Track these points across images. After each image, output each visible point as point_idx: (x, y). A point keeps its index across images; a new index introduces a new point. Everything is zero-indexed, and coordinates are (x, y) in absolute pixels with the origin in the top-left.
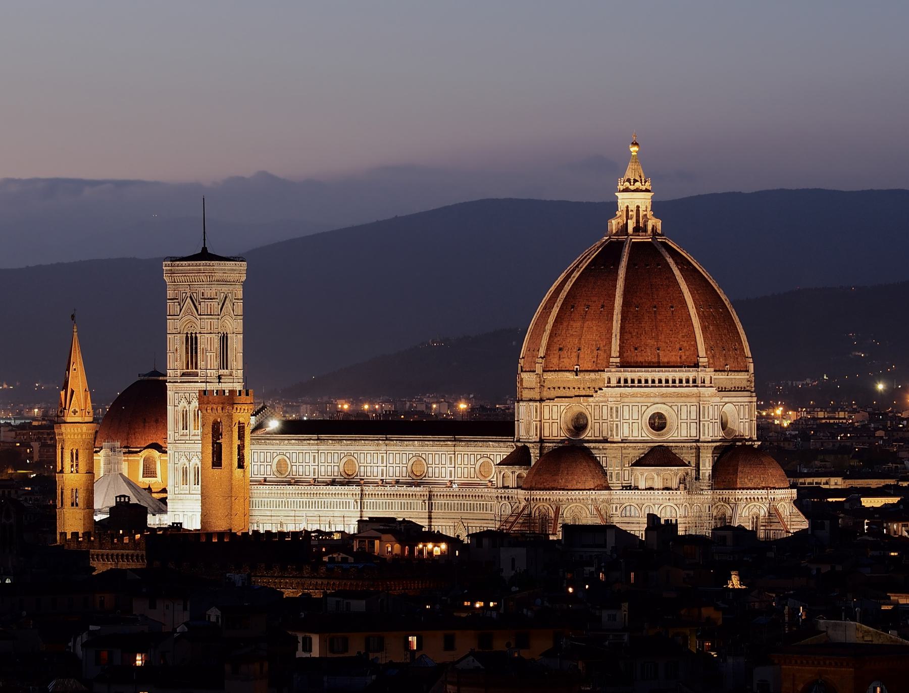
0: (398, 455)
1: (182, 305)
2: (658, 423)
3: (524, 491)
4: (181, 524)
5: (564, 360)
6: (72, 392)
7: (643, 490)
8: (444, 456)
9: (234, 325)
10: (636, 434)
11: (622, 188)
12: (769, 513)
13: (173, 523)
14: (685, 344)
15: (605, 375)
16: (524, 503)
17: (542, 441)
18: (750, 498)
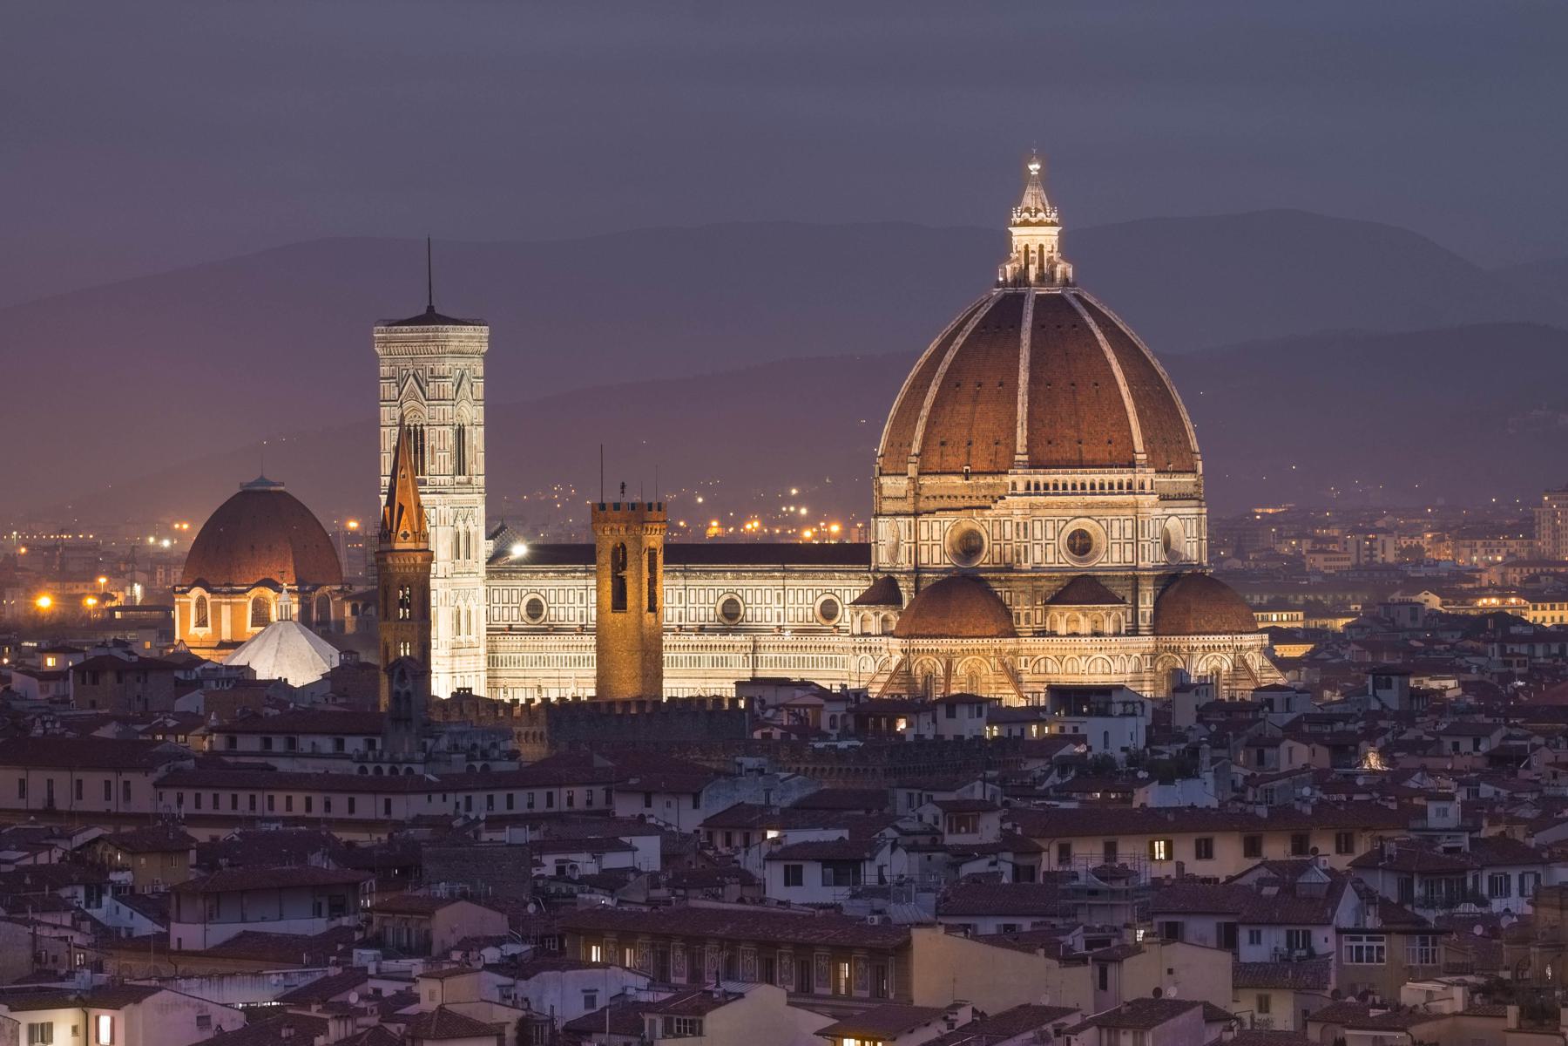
0: (702, 592)
1: (401, 386)
2: (1081, 544)
3: (900, 640)
4: (470, 689)
5: (948, 458)
6: (401, 508)
7: (1064, 636)
8: (768, 592)
9: (472, 413)
10: (1050, 559)
11: (1018, 220)
12: (1234, 666)
13: (459, 689)
14: (1116, 435)
15: (1008, 479)
16: (898, 657)
17: (918, 570)
18: (1209, 647)
